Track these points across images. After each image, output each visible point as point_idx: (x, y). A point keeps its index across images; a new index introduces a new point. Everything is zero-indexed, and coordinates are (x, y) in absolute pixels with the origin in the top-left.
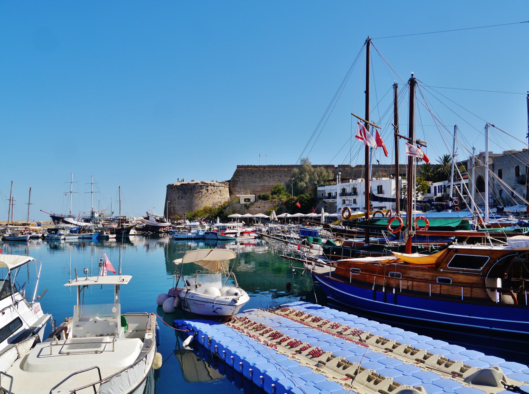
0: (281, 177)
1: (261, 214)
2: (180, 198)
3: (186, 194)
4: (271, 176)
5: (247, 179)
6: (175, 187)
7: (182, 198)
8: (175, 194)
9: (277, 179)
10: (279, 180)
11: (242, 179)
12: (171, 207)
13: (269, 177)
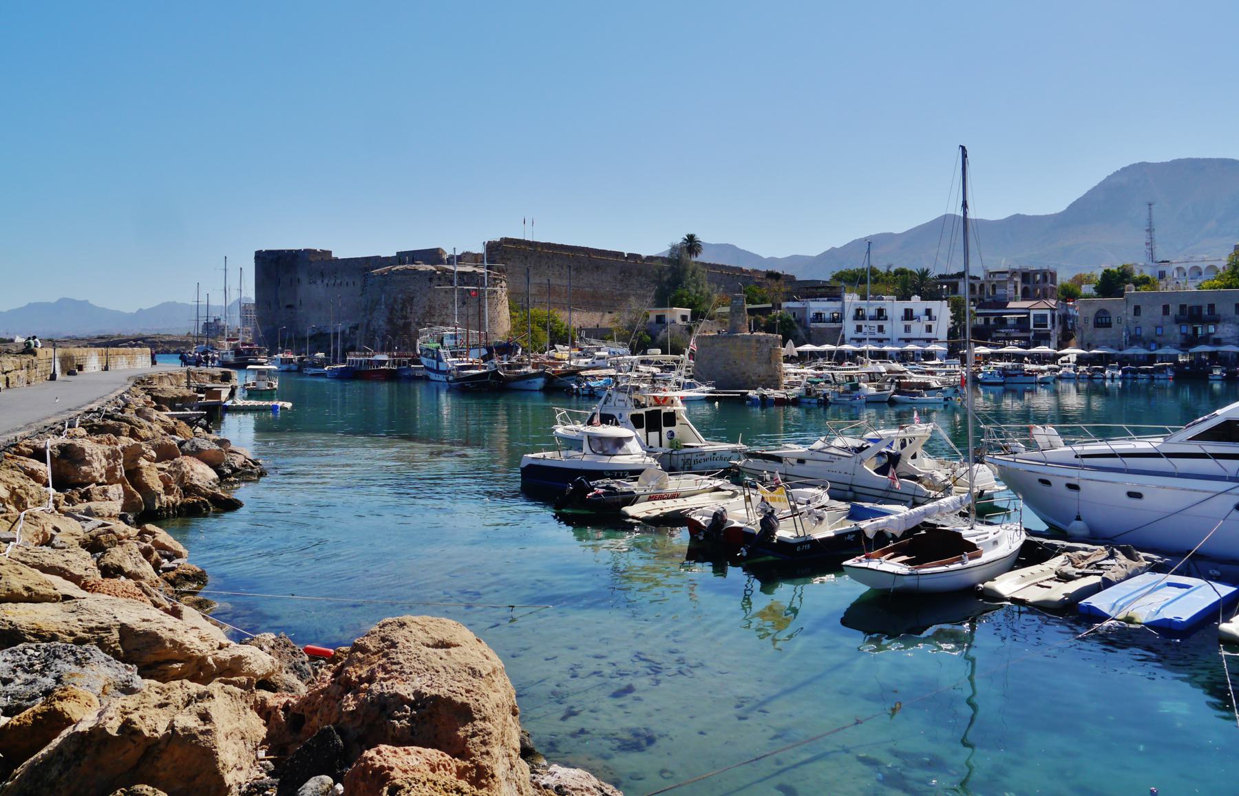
5: (518, 269)
6: (442, 277)
9: (557, 273)
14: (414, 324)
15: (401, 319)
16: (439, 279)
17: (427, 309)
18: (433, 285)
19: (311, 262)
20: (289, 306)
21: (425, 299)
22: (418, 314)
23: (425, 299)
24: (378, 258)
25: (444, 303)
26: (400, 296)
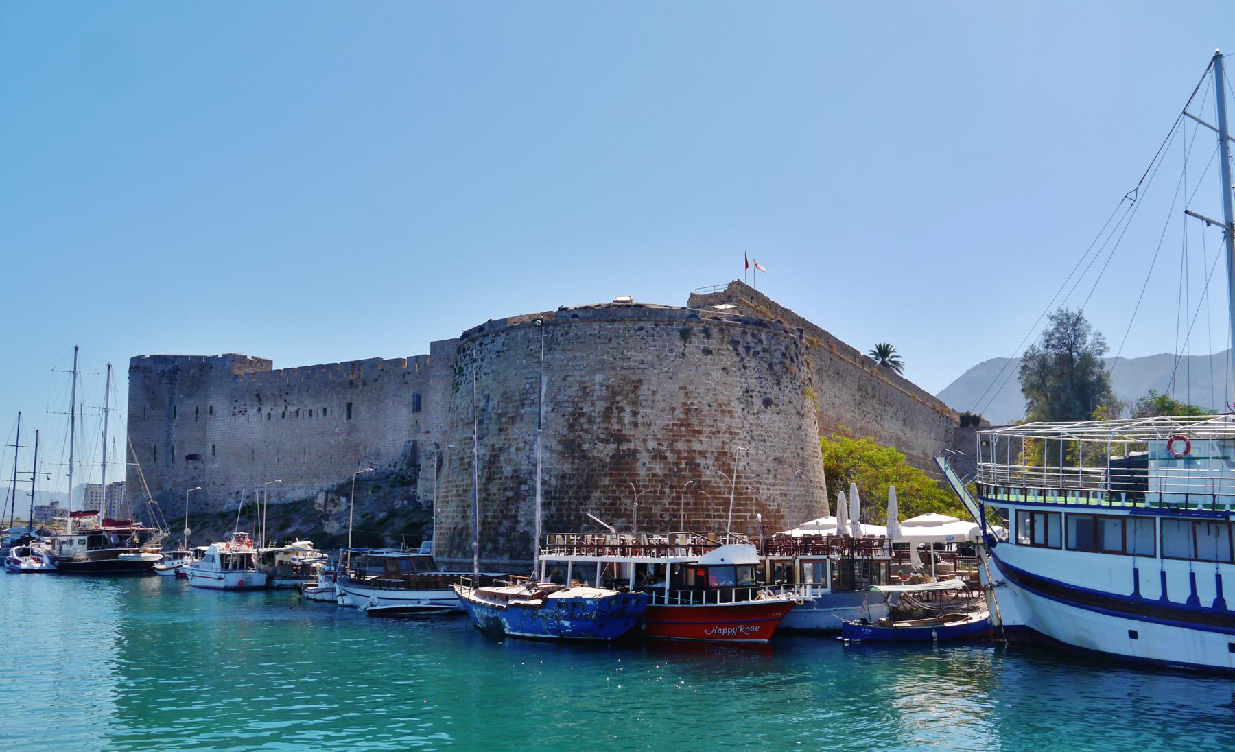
1: (934, 517)
2: (758, 403)
3: (778, 383)
7: (767, 403)
8: (716, 375)
12: (703, 454)
14: (644, 457)
15: (606, 441)
16: (707, 333)
17: (679, 413)
19: (237, 376)
20: (191, 457)
21: (673, 387)
22: (655, 428)
23: (673, 387)
24: (378, 360)
25: (721, 399)
26: (599, 378)
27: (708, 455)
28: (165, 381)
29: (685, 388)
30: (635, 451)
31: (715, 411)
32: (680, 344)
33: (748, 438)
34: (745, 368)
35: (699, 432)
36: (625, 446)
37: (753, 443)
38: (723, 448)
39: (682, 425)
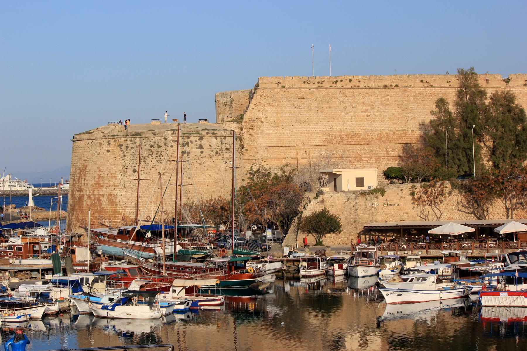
0: (373, 108)
2: (130, 171)
4: (348, 104)
5: (287, 115)
9: (363, 114)
10: (368, 115)
11: (275, 114)
12: (103, 196)
13: (341, 107)
18: (103, 150)
25: (112, 171)
27: (105, 196)
28: (227, 108)
29: (98, 168)
30: (84, 195)
31: (109, 177)
32: (98, 148)
33: (123, 188)
34: (125, 156)
35: (102, 186)
36: (81, 193)
37: (125, 190)
38: (111, 193)
39: (97, 184)
